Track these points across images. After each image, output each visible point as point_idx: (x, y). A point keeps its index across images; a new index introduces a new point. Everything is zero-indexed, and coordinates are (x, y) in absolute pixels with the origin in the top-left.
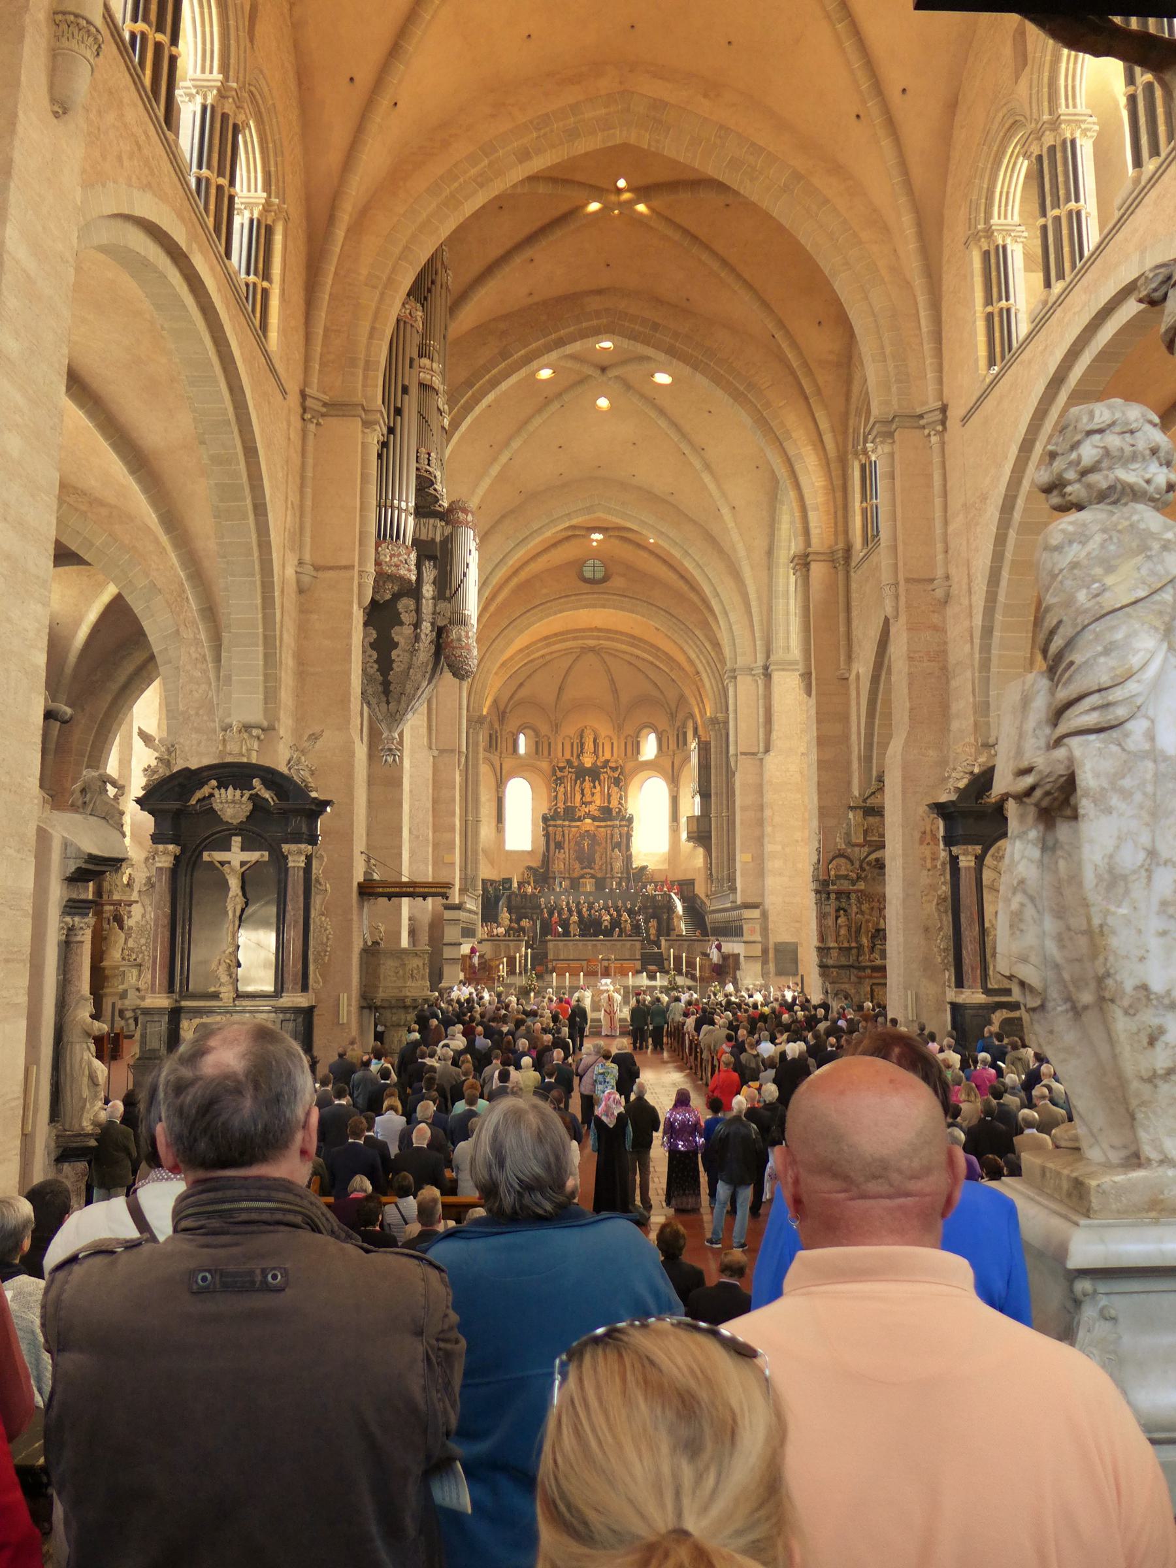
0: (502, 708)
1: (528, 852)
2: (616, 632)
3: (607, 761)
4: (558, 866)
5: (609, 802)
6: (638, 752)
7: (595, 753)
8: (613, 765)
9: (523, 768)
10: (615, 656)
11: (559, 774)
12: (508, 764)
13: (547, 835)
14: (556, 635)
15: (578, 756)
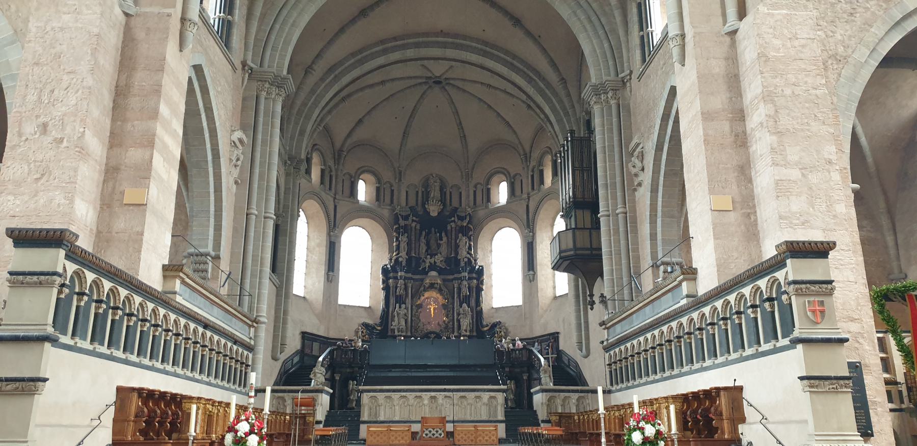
0: (338, 145)
1: (365, 308)
2: (465, 37)
3: (456, 209)
4: (398, 323)
5: (457, 253)
6: (489, 200)
7: (443, 201)
8: (463, 215)
9: (359, 213)
10: (464, 91)
11: (402, 223)
12: (343, 208)
13: (386, 288)
14: (395, 39)
15: (423, 205)
